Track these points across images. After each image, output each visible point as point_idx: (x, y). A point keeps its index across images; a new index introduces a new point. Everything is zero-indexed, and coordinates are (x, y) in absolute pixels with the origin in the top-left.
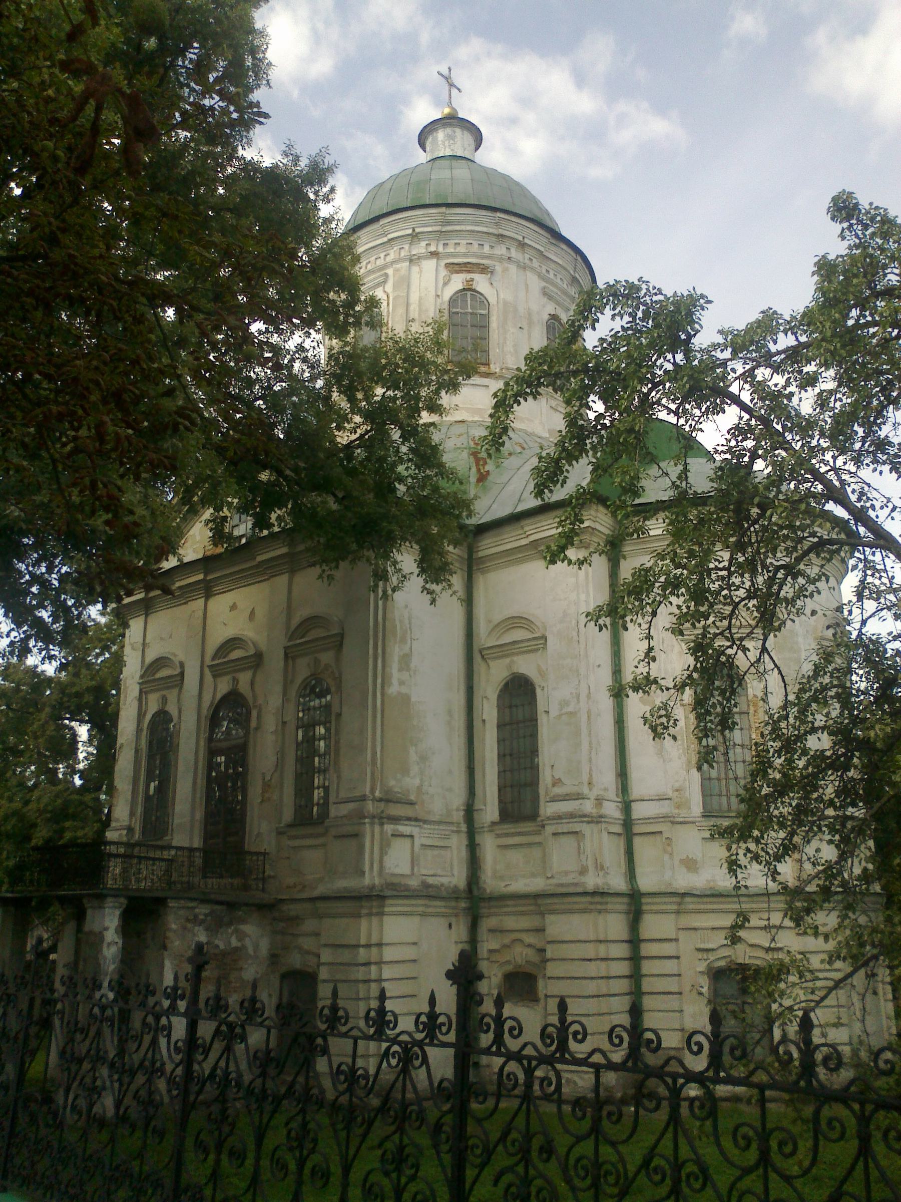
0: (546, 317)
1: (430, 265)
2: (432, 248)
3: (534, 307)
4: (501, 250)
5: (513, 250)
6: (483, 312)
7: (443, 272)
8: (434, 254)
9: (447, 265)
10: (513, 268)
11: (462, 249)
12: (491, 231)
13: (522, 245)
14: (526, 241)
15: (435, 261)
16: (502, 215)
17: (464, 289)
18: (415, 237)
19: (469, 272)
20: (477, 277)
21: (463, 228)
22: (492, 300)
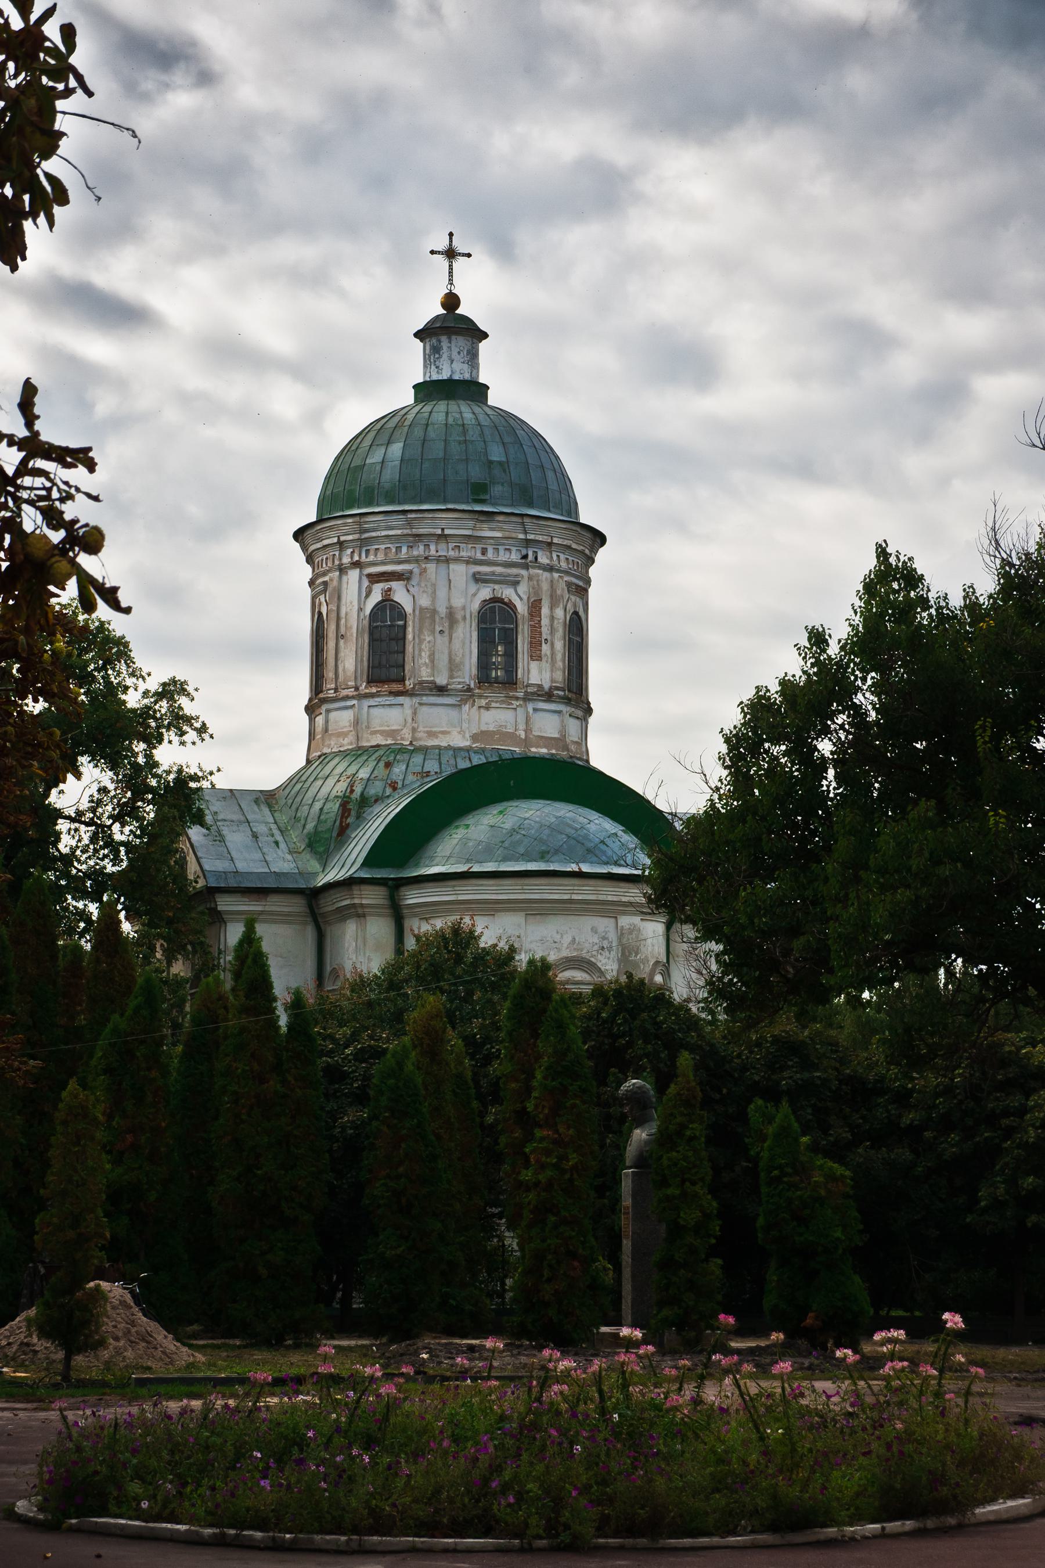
0: (476, 606)
1: (354, 575)
2: (356, 558)
3: (458, 602)
4: (419, 550)
5: (433, 547)
6: (401, 623)
7: (366, 583)
8: (357, 565)
9: (369, 576)
10: (431, 567)
11: (381, 557)
12: (406, 532)
13: (443, 537)
14: (447, 532)
15: (358, 570)
16: (413, 516)
17: (383, 601)
18: (341, 545)
19: (387, 581)
20: (394, 585)
21: (378, 534)
22: (409, 609)
